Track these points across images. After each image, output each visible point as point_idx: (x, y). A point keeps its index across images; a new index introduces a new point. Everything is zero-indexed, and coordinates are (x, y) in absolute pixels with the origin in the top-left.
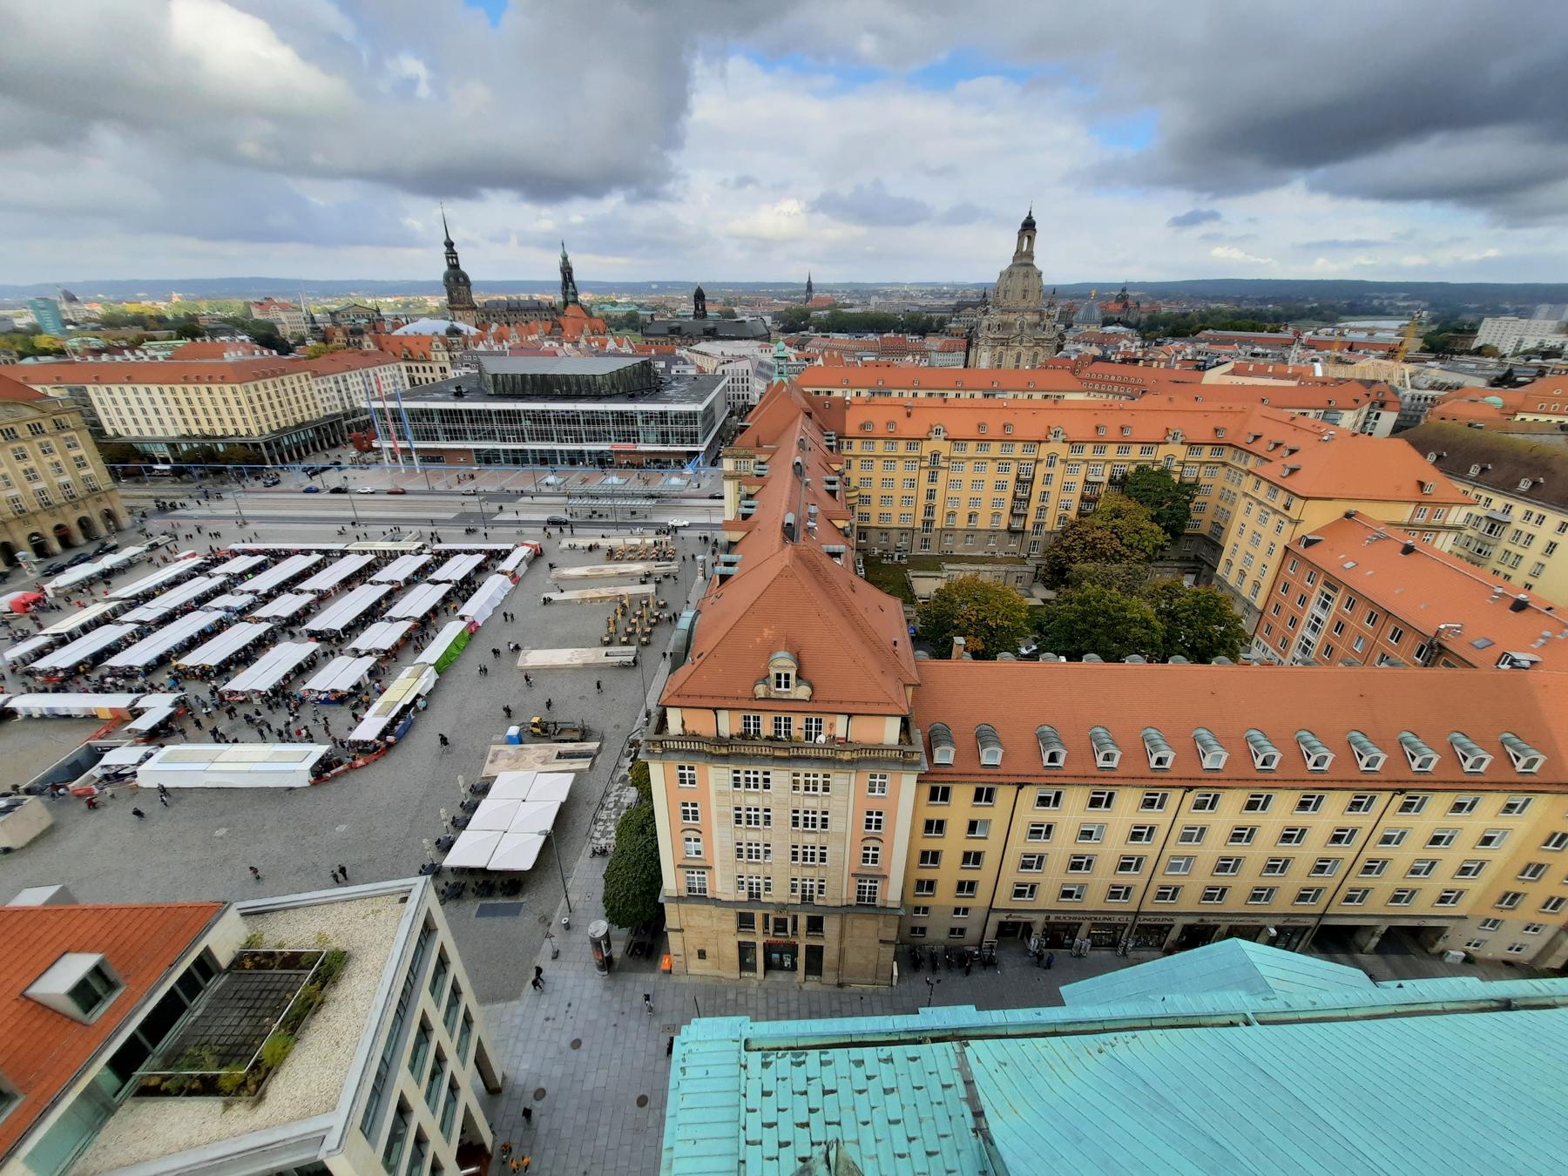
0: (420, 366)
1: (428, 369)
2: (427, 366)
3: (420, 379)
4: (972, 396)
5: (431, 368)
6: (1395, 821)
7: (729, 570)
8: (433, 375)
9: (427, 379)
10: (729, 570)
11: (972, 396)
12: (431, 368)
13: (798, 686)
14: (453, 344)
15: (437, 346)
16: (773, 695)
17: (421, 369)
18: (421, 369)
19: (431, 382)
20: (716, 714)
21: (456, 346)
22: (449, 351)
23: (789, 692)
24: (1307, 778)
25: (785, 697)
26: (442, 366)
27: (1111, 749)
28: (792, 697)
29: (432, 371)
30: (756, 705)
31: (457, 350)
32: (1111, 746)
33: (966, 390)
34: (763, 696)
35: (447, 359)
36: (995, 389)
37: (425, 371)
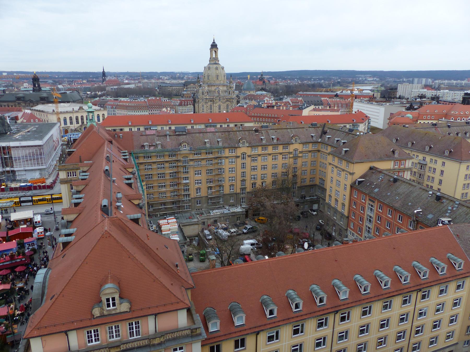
4: (139, 129)
6: (341, 327)
7: (69, 239)
10: (69, 239)
11: (139, 129)
13: (121, 304)
16: (105, 313)
20: (67, 335)
23: (116, 309)
24: (236, 331)
25: (113, 312)
27: (272, 307)
28: (118, 311)
30: (94, 322)
32: (272, 305)
33: (134, 126)
34: (99, 315)
36: (151, 125)
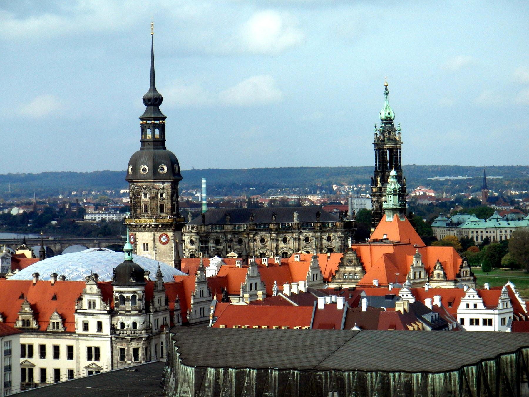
0: (50, 343)
1: (63, 352)
2: (63, 343)
3: (43, 371)
5: (70, 349)
8: (71, 364)
9: (57, 372)
12: (70, 349)
14: (123, 300)
15: (92, 305)
17: (50, 351)
18: (50, 351)
19: (64, 377)
21: (129, 305)
22: (112, 313)
26: (93, 344)
29: (70, 356)
31: (128, 314)
35: (106, 329)
37: (57, 355)
